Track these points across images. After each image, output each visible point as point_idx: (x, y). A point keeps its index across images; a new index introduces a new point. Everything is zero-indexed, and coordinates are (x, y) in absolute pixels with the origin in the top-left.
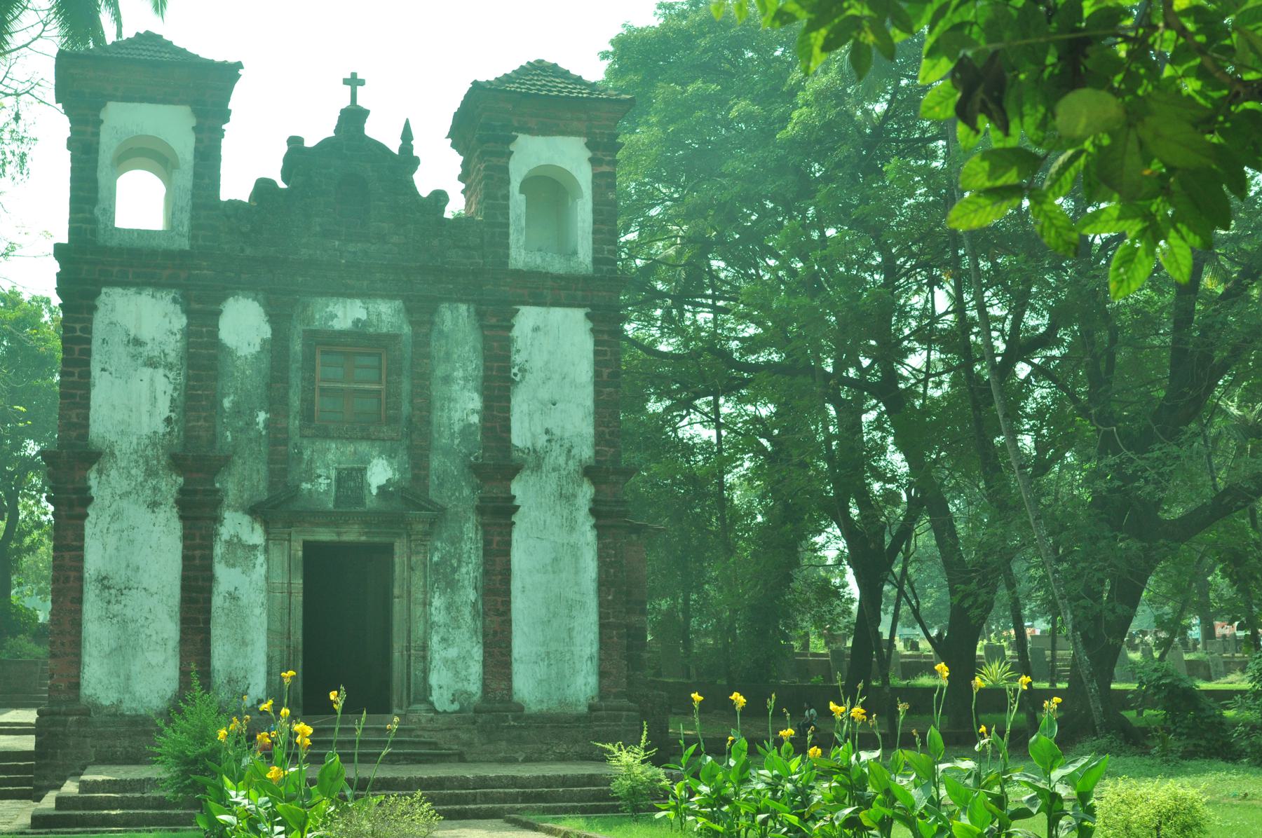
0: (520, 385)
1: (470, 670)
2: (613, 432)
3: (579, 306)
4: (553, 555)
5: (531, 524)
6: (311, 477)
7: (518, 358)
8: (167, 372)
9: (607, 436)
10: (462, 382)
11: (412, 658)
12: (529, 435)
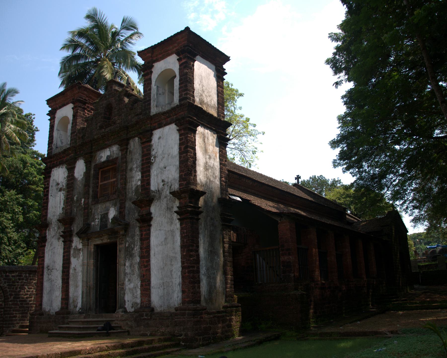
0: (154, 164)
1: (137, 293)
2: (185, 174)
4: (165, 237)
5: (157, 223)
6: (94, 221)
7: (153, 153)
9: (184, 177)
10: (135, 169)
12: (156, 184)
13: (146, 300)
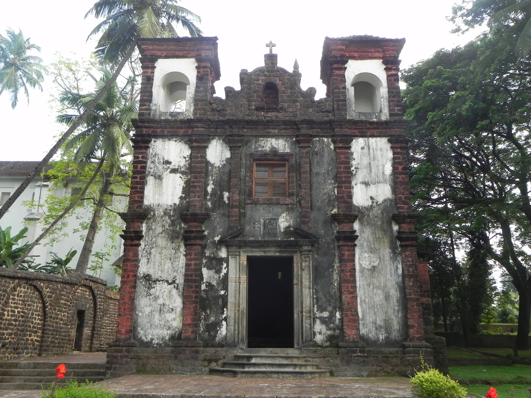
3: (384, 136)
8: (181, 176)
9: (403, 199)
11: (304, 317)
13: (354, 333)
